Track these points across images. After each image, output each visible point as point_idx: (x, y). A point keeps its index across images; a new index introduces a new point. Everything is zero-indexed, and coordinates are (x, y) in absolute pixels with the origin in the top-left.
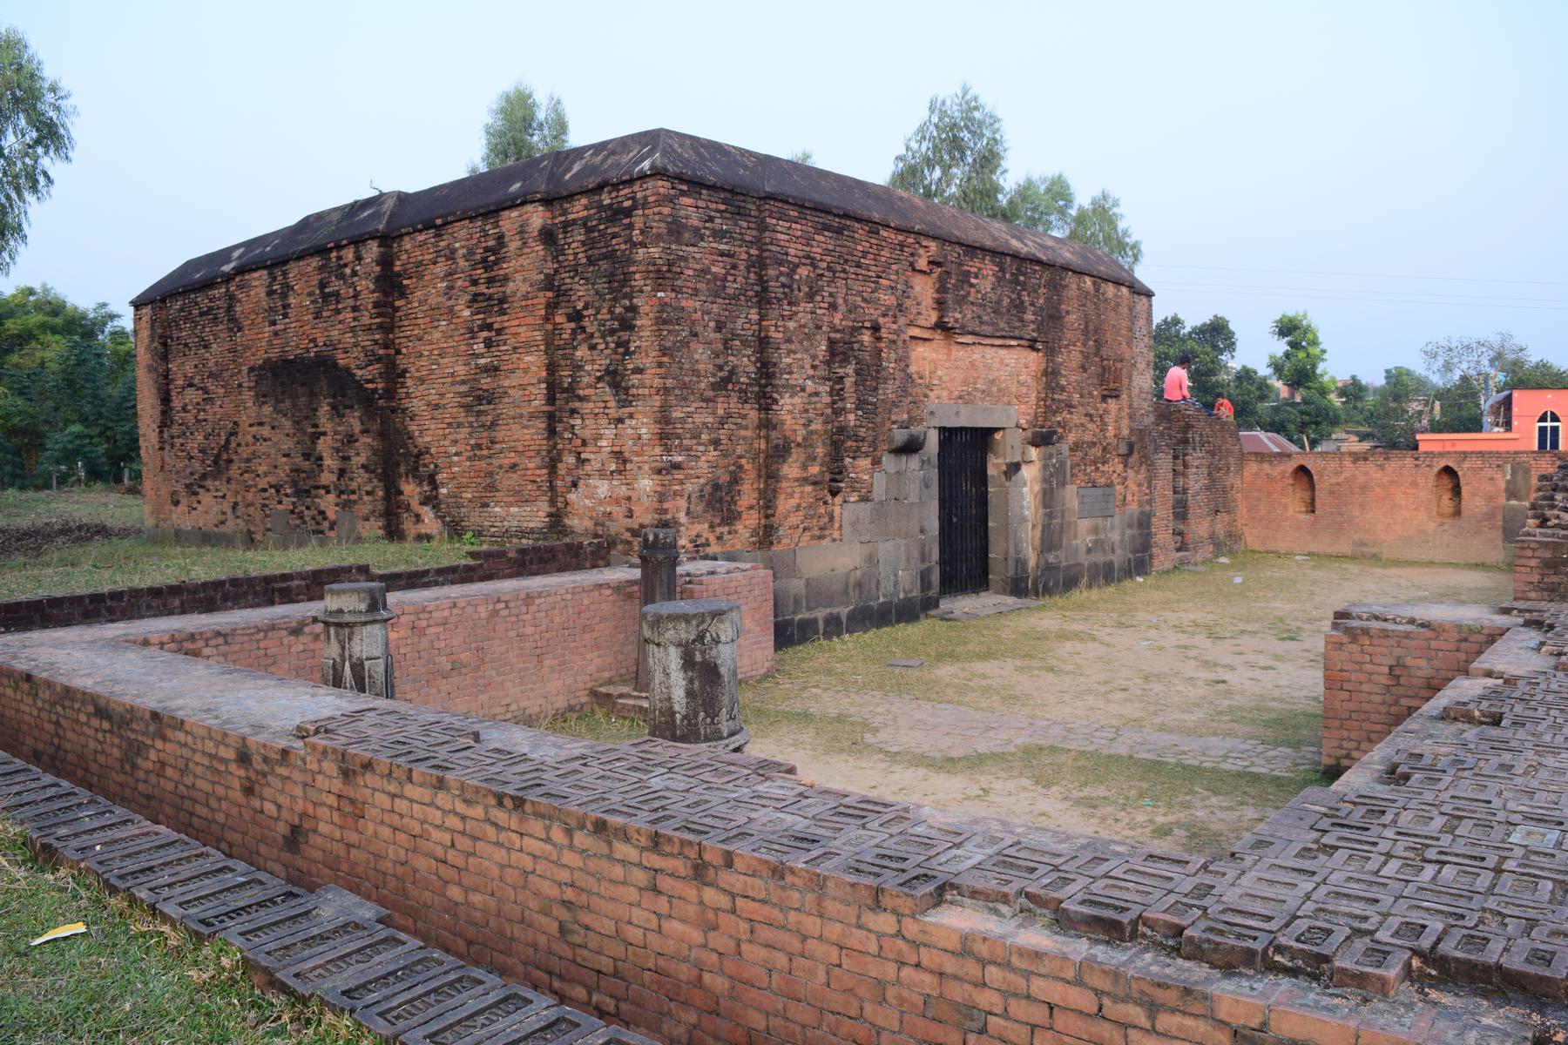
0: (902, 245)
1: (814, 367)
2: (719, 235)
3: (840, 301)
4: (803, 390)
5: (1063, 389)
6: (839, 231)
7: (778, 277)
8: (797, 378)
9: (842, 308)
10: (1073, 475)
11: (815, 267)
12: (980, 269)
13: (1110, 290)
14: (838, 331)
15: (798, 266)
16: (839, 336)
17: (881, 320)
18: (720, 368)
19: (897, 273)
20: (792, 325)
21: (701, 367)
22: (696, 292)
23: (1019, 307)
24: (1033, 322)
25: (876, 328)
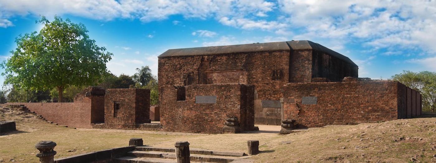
0: (199, 58)
1: (180, 80)
2: (167, 63)
3: (185, 69)
4: (178, 83)
5: (254, 78)
6: (185, 59)
7: (173, 68)
8: (177, 81)
9: (186, 70)
10: (259, 97)
11: (180, 65)
12: (221, 58)
13: (278, 54)
14: (185, 74)
15: (177, 65)
16: (185, 75)
17: (194, 71)
18: (167, 81)
19: (198, 63)
20: (176, 74)
21: (164, 81)
22: (163, 71)
23: (236, 63)
24: (241, 66)
25: (193, 72)
